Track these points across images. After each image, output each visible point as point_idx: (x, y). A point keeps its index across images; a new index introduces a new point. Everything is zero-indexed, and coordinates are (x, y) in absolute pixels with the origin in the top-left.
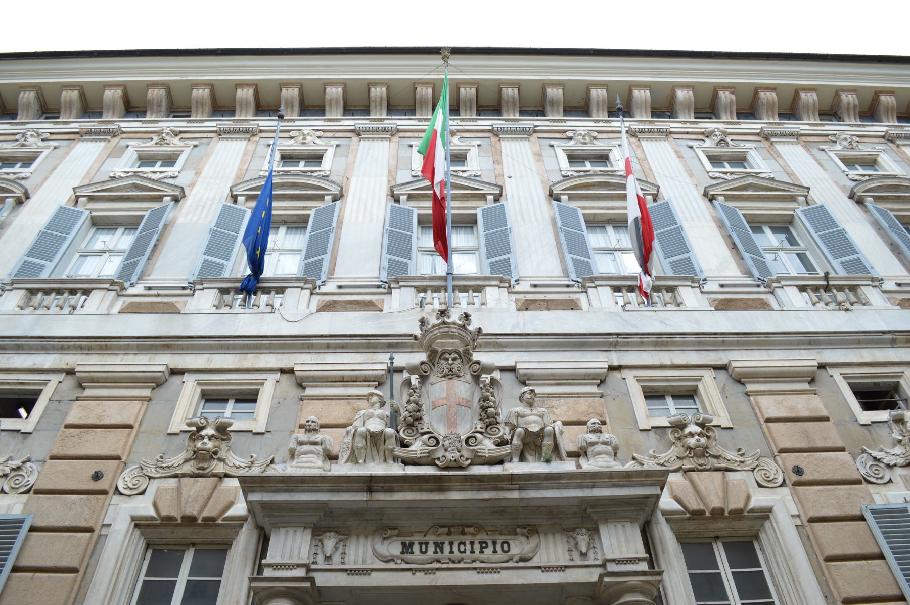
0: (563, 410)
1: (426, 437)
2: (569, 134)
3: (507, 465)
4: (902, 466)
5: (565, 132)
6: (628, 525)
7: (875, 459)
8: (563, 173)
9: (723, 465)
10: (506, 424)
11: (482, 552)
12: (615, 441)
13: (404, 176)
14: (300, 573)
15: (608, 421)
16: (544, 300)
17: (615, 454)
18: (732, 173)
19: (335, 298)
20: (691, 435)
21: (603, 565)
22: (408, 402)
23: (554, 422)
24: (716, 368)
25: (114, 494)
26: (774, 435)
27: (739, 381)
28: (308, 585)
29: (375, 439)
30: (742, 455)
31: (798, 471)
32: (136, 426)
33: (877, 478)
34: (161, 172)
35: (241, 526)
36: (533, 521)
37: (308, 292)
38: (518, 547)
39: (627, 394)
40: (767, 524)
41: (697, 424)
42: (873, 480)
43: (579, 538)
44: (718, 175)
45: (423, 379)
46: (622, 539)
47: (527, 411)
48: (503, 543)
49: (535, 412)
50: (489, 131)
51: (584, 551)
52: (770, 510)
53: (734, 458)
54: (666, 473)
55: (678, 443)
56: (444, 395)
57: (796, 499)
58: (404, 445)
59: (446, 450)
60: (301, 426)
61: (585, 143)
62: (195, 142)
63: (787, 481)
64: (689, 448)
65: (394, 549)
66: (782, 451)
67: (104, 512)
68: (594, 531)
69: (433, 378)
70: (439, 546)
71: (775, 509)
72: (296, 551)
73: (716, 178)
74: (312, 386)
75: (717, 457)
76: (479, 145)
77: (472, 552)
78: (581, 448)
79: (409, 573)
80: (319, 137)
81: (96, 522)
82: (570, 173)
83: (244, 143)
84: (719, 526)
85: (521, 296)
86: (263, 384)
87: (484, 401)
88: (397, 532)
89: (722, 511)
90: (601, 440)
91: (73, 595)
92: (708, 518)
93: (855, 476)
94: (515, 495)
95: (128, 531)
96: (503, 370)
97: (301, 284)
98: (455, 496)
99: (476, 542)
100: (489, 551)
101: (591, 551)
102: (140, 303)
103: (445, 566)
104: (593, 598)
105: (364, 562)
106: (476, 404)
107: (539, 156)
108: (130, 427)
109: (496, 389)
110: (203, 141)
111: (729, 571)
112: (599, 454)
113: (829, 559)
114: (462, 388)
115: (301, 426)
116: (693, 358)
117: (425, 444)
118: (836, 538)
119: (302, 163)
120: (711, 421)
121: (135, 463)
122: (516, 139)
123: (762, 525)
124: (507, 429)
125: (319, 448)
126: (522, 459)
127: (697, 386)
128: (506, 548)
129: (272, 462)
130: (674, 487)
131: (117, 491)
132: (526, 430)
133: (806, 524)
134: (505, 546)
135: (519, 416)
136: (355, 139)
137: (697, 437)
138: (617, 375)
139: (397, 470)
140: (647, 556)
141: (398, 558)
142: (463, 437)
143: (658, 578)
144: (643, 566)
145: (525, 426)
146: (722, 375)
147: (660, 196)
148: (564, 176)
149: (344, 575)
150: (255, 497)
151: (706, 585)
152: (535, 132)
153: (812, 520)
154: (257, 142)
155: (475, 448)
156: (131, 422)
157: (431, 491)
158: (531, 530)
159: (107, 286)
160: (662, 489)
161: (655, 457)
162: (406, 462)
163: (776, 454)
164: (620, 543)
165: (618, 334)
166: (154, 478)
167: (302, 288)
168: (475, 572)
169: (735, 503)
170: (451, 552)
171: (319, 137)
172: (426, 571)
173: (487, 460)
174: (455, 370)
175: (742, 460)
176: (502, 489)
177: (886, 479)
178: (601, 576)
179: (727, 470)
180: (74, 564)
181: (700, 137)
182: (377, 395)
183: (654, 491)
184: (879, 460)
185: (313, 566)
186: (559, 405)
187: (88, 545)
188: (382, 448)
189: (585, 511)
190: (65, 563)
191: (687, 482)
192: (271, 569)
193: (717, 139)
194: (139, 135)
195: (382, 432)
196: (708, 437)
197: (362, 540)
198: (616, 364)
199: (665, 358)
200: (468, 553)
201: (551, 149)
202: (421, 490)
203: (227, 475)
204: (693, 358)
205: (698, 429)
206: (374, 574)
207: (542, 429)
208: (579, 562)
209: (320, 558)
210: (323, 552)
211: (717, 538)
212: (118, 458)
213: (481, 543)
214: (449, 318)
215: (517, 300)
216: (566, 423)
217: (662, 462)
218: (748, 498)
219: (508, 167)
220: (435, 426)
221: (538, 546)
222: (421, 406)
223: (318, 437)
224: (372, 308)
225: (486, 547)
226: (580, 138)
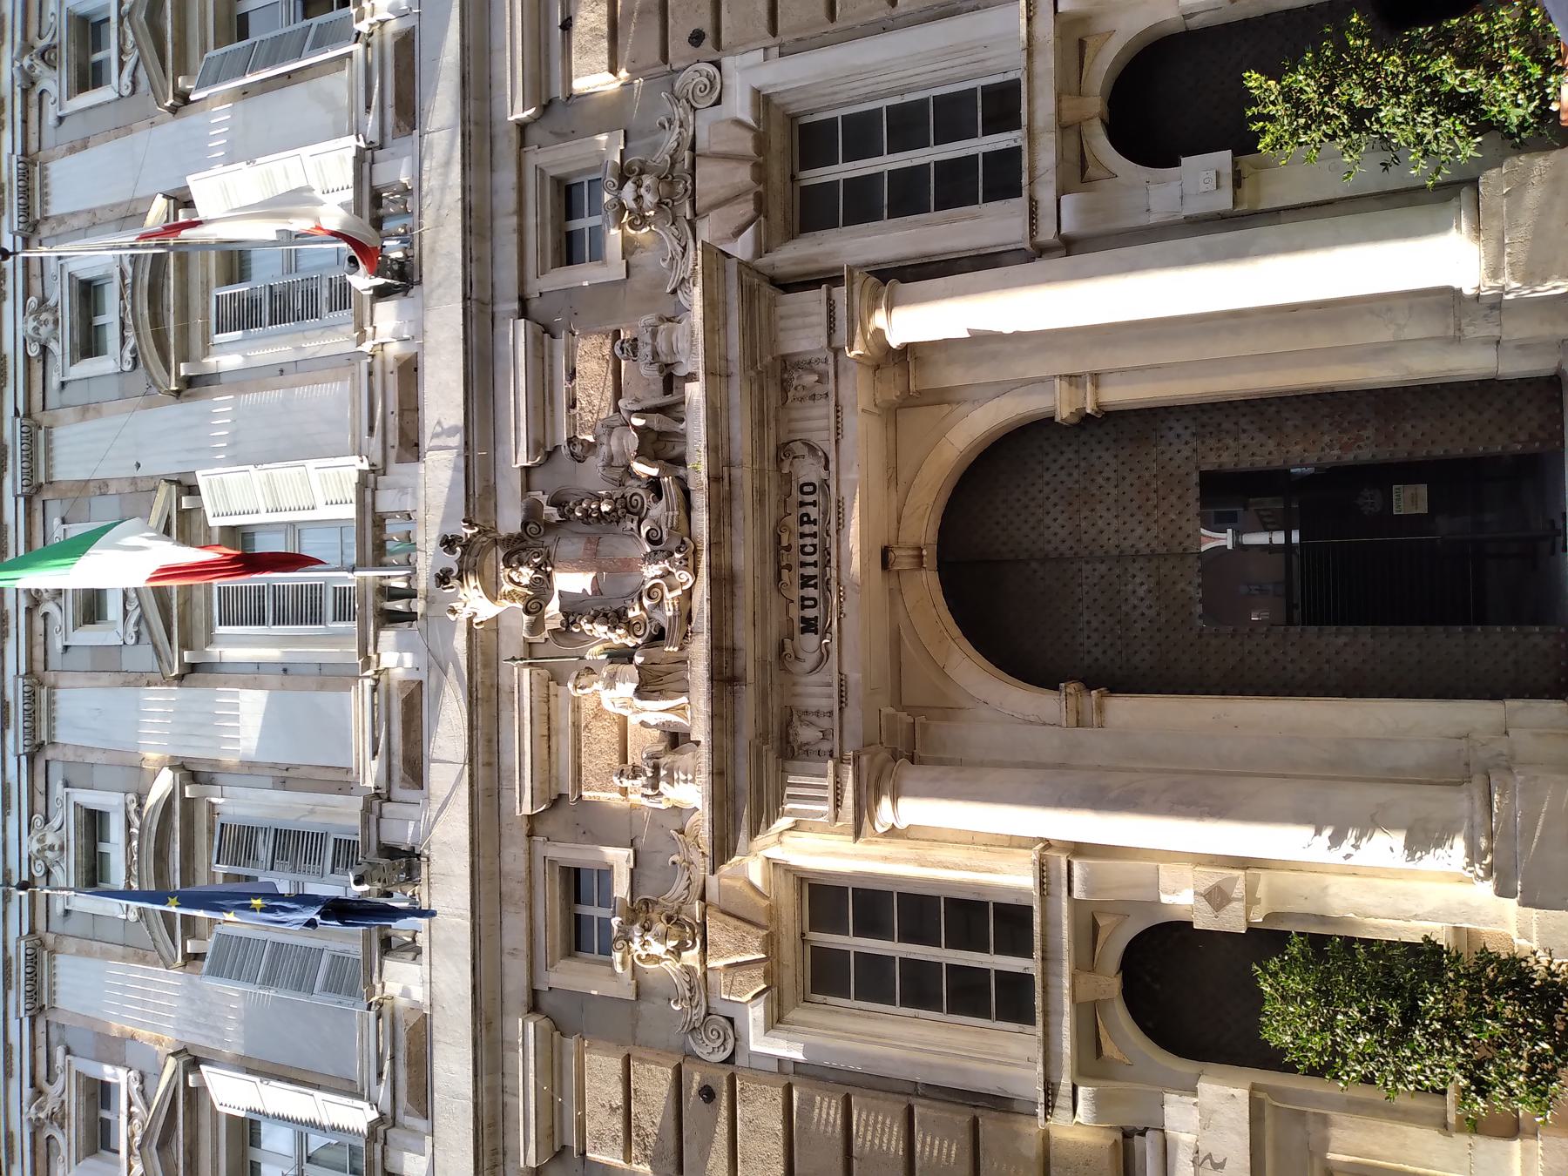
2: (34, 351)
5: (27, 358)
6: (781, 310)
8: (127, 367)
9: (687, 154)
10: (622, 484)
11: (815, 522)
13: (142, 657)
15: (614, 327)
16: (401, 415)
17: (669, 320)
18: (121, 51)
19: (397, 762)
20: (638, 198)
23: (617, 409)
24: (523, 143)
30: (670, 122)
31: (697, 38)
34: (130, 1104)
36: (773, 449)
37: (387, 807)
39: (568, 292)
40: (776, 100)
41: (621, 188)
43: (795, 383)
44: (126, 79)
46: (799, 321)
47: (604, 449)
48: (803, 493)
49: (604, 439)
50: (29, 501)
51: (816, 378)
52: (757, 92)
53: (675, 137)
61: (56, 322)
62: (59, 1052)
63: (714, 58)
64: (659, 205)
70: (805, 582)
73: (134, 83)
76: (64, 522)
77: (814, 535)
78: (661, 372)
79: (844, 621)
80: (47, 821)
82: (128, 356)
83: (60, 960)
84: (777, 171)
85: (392, 454)
86: (552, 862)
88: (787, 641)
89: (756, 165)
92: (766, 190)
95: (789, 1031)
96: (527, 487)
97: (373, 818)
99: (801, 529)
100: (814, 513)
101: (815, 366)
102: (410, 1086)
103: (834, 573)
104: (877, 367)
105: (830, 685)
107: (86, 410)
109: (566, 498)
110: (54, 1037)
111: (841, 166)
113: (832, 15)
116: (506, 177)
119: (103, 847)
122: (48, 451)
123: (778, 107)
126: (680, 461)
130: (719, 234)
131: (730, 1060)
133: (778, 40)
134: (806, 489)
135: (609, 463)
136: (50, 753)
137: (643, 191)
138: (534, 305)
139: (700, 648)
144: (840, 293)
146: (534, 134)
147: (177, 194)
148: (135, 366)
149: (847, 712)
151: (862, 204)
152: (28, 414)
153: (773, 31)
154: (58, 935)
155: (665, 530)
159: (378, 1147)
160: (728, 256)
161: (673, 258)
165: (465, 298)
166: (708, 1007)
167: (380, 816)
169: (746, 144)
170: (815, 564)
171: (47, 821)
173: (683, 513)
175: (677, 123)
179: (693, 148)
181: (34, 97)
185: (836, 754)
189: (759, 373)
193: (40, 67)
194: (41, 1165)
196: (642, 172)
197: (799, 689)
198: (516, 306)
199: (506, 224)
200: (816, 541)
201: (68, 387)
204: (506, 177)
205: (629, 187)
206: (845, 670)
209: (825, 746)
211: (793, 177)
212: (678, 1071)
213: (802, 523)
214: (451, 571)
215: (400, 460)
217: (679, 249)
218: (739, 123)
219: (116, 468)
220: (629, 590)
221: (806, 444)
224: (416, 700)
225: (808, 515)
226: (43, 331)
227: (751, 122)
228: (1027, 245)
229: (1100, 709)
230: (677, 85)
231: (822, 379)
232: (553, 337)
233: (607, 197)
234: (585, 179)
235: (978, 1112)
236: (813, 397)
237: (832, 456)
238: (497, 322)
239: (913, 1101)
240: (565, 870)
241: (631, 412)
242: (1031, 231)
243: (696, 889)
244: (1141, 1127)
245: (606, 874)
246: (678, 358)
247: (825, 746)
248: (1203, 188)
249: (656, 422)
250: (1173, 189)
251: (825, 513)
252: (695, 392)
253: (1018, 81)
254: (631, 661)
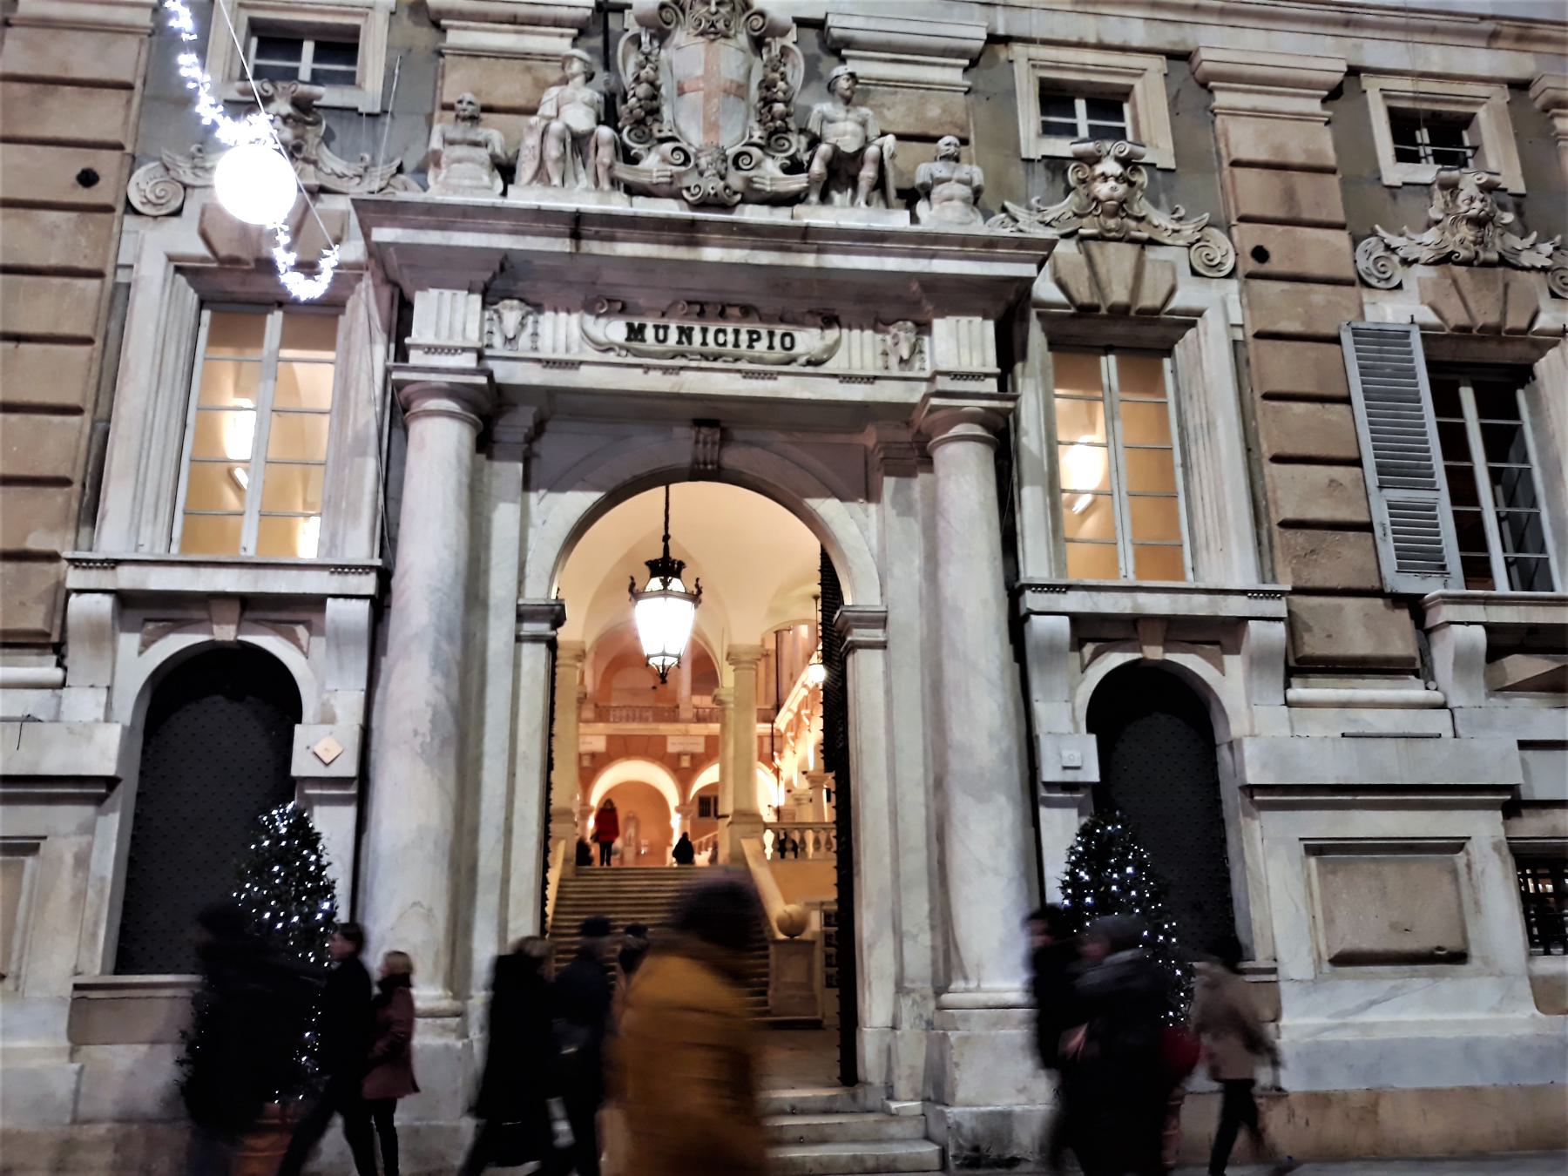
0: (900, 115)
1: (668, 146)
3: (798, 209)
4: (1426, 264)
7: (1388, 247)
9: (1145, 235)
10: (802, 131)
11: (750, 346)
12: (978, 179)
14: (469, 361)
15: (972, 138)
17: (975, 203)
21: (931, 380)
22: (637, 79)
23: (883, 134)
25: (125, 212)
26: (1239, 191)
27: (1204, 85)
28: (483, 380)
29: (578, 143)
30: (1180, 219)
31: (1260, 254)
32: (138, 84)
33: (1380, 280)
35: (359, 278)
38: (809, 340)
39: (1011, 93)
40: (1190, 334)
41: (1117, 159)
42: (1373, 281)
43: (902, 334)
45: (661, 35)
48: (784, 335)
51: (906, 356)
52: (1200, 314)
54: (1051, 244)
55: (1081, 188)
56: (699, 72)
57: (1245, 301)
58: (632, 160)
59: (701, 174)
60: (448, 107)
64: (1095, 199)
65: (616, 330)
66: (1243, 219)
67: (114, 244)
68: (923, 328)
69: (680, 36)
70: (685, 333)
71: (1207, 313)
72: (458, 326)
74: (458, 28)
75: (1140, 219)
77: (736, 345)
79: (640, 371)
81: (105, 262)
87: (768, 88)
89: (1127, 308)
90: (956, 176)
91: (93, 381)
92: (1103, 317)
93: (1351, 274)
94: (809, 260)
95: (165, 280)
96: (802, 23)
98: (711, 254)
100: (761, 346)
101: (918, 357)
103: (693, 364)
105: (568, 350)
106: (754, 94)
108: (129, 87)
112: (950, 199)
114: (731, 59)
115: (448, 107)
117: (664, 160)
118: (1283, 367)
120: (1142, 157)
121: (154, 159)
124: (804, 140)
125: (483, 154)
127: (1132, 87)
128: (788, 344)
129: (400, 169)
130: (1060, 263)
131: (130, 209)
132: (836, 149)
133: (1250, 339)
134: (788, 340)
135: (825, 119)
137: (1112, 183)
138: (1003, 53)
139: (619, 204)
140: (998, 370)
141: (621, 347)
142: (731, 152)
143: (1010, 405)
144: (991, 386)
145: (833, 140)
149: (538, 367)
150: (383, 234)
155: (751, 173)
156: (126, 77)
157: (676, 243)
158: (829, 320)
160: (1039, 269)
161: (1039, 211)
162: (632, 190)
163: (1234, 222)
164: (962, 343)
166: (194, 187)
168: (738, 376)
169: (1149, 299)
170: (704, 343)
172: (666, 370)
174: (721, 25)
175: (1177, 227)
176: (787, 249)
177: (1395, 282)
178: (927, 397)
180: (85, 331)
182: (581, 59)
183: (1028, 270)
184: (1394, 251)
186: (894, 104)
187: (100, 300)
188: (591, 161)
190: (66, 329)
191: (1082, 258)
192: (420, 352)
195: (592, 132)
198: (1001, 31)
200: (730, 347)
202: (659, 242)
203: (323, 190)
205: (1116, 169)
206: (583, 368)
207: (861, 151)
208: (895, 372)
209: (497, 340)
210: (502, 331)
211: (1107, 350)
212: (118, 147)
213: (750, 333)
216: (900, 137)
217: (1048, 219)
220: (682, 125)
221: (837, 343)
222: (658, 88)
223: (480, 133)
225: (759, 339)
227: (1172, 305)
228: (1023, 580)
229: (535, 639)
230: (1215, 231)
231: (901, 360)
232: (966, 69)
233: (1108, 145)
234: (1128, 124)
235: (77, 487)
236: (885, 354)
237: (821, 370)
238: (985, 9)
239: (87, 416)
240: (355, 32)
241: (881, 148)
242: (1037, 586)
243: (331, 183)
244: (67, 662)
245: (349, 79)
246: (936, 207)
247: (497, 340)
248: (1066, 753)
249: (868, 173)
250: (1065, 726)
251: (760, 360)
252: (898, 220)
253: (1182, 577)
254: (599, 123)
